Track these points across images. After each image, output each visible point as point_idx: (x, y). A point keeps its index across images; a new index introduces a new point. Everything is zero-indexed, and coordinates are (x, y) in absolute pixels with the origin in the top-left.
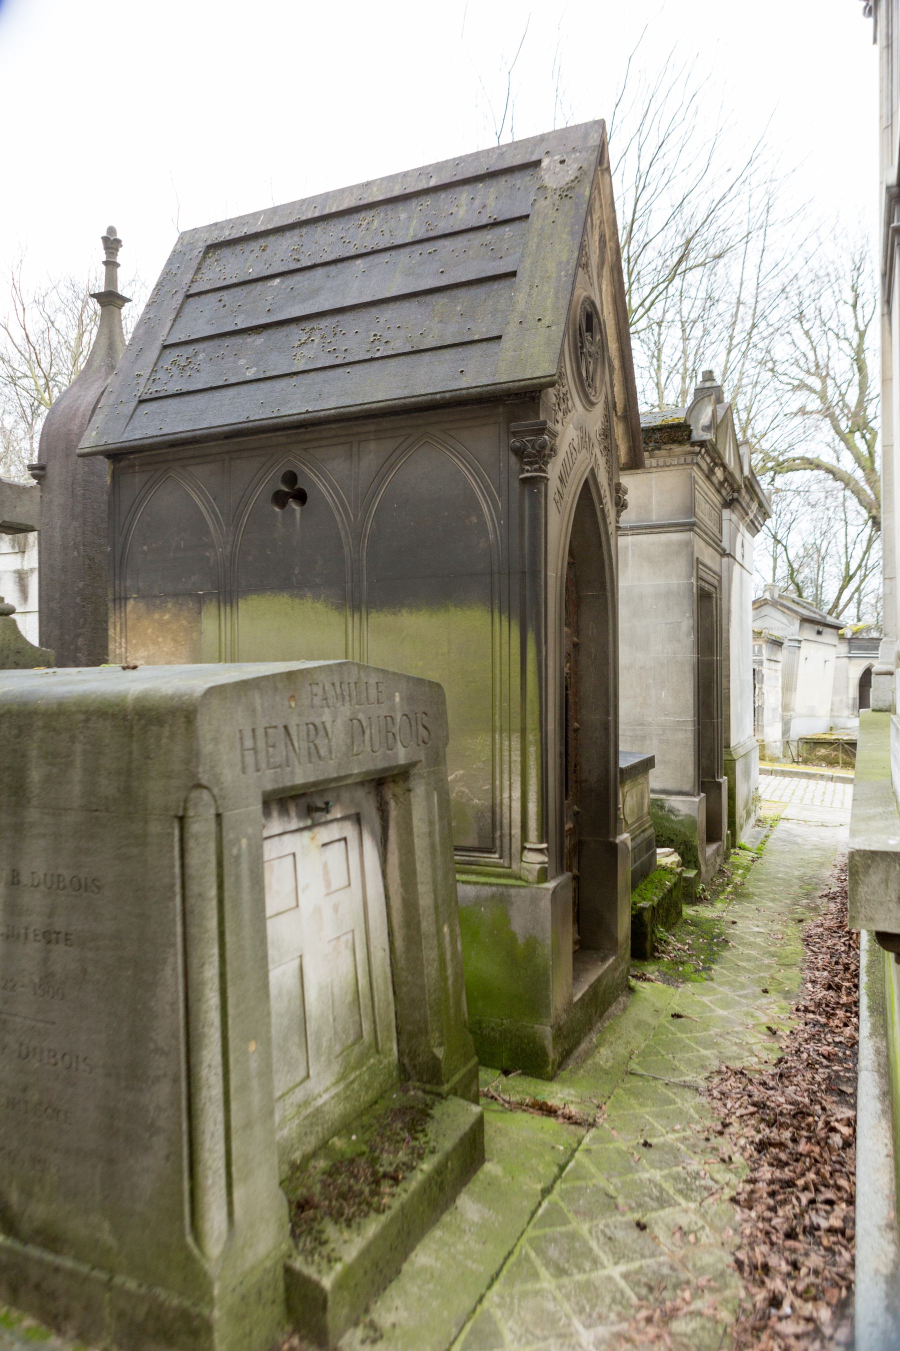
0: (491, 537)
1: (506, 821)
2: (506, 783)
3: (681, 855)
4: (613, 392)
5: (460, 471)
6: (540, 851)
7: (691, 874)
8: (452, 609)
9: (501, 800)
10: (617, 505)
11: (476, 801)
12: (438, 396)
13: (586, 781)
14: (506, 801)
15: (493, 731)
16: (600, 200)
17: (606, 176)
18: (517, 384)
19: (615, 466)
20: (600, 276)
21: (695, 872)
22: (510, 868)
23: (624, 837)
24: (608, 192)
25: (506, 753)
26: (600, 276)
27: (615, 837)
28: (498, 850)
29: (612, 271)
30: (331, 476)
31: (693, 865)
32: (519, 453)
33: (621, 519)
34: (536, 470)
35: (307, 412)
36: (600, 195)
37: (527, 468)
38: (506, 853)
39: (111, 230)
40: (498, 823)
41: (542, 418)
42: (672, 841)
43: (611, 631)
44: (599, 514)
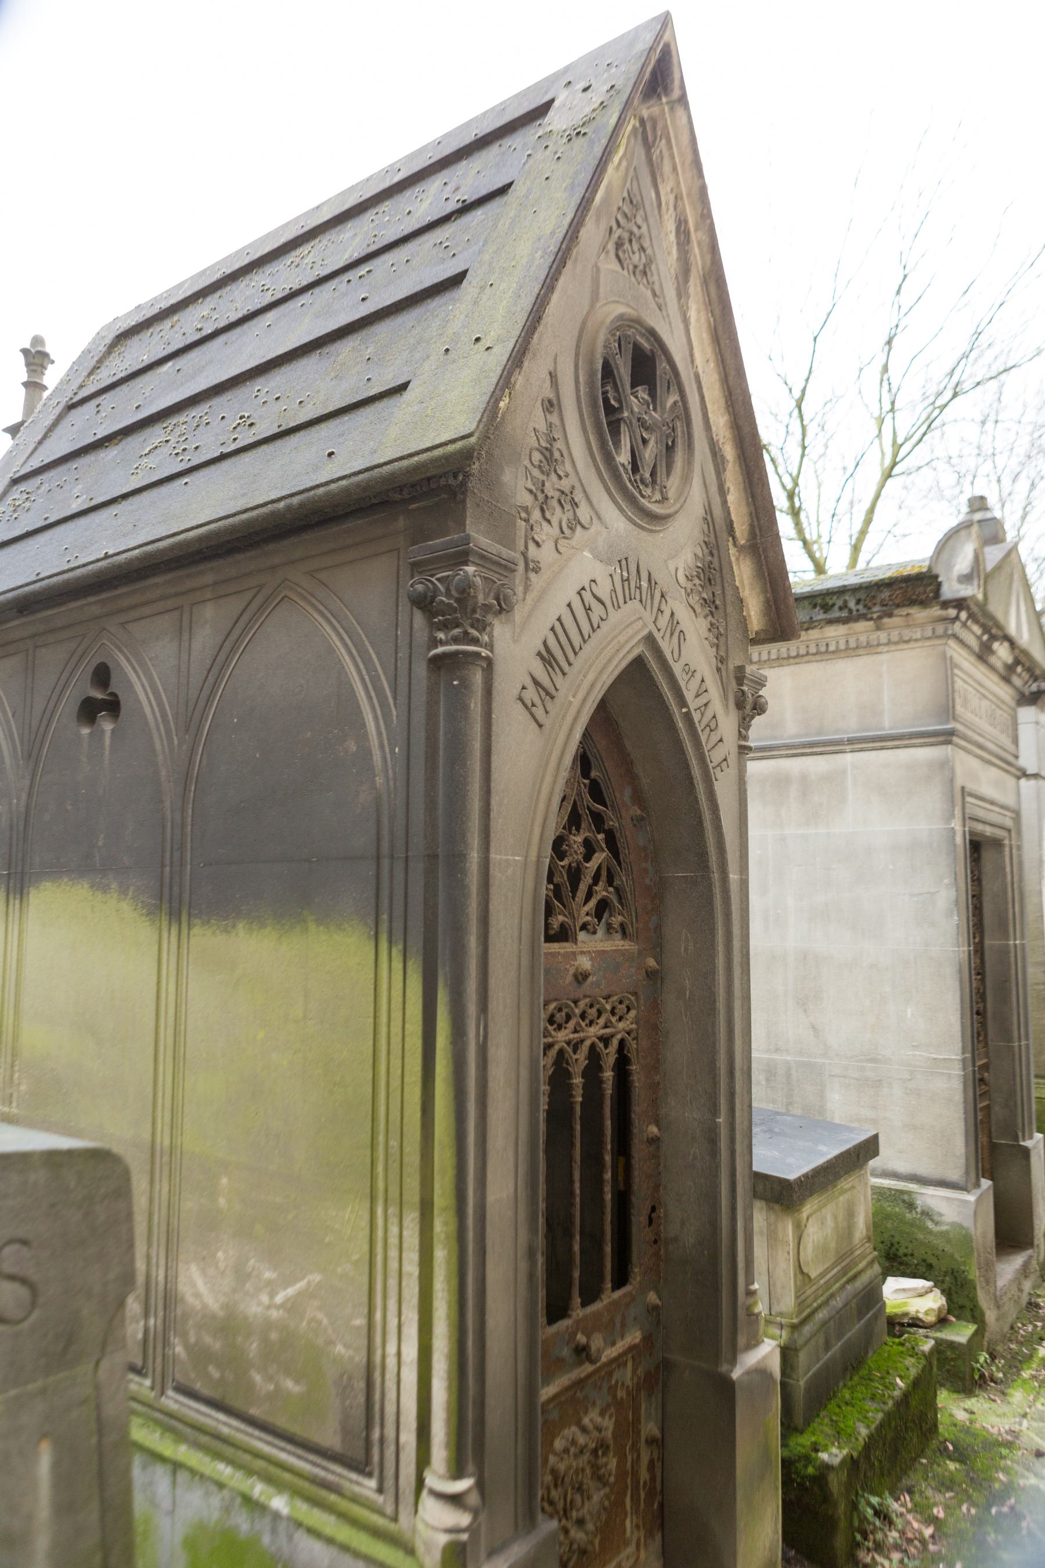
0: (379, 780)
1: (390, 1409)
2: (393, 1322)
3: (947, 1293)
4: (725, 502)
5: (334, 649)
6: (455, 1500)
7: (961, 1333)
8: (312, 926)
9: (384, 1357)
10: (740, 705)
11: (339, 1349)
12: (282, 504)
13: (676, 1239)
14: (391, 1362)
15: (373, 1199)
16: (672, 157)
17: (680, 112)
18: (405, 463)
19: (734, 636)
20: (682, 293)
21: (972, 1328)
22: (395, 1519)
23: (765, 1353)
24: (685, 139)
25: (393, 1253)
26: (682, 293)
27: (733, 1362)
28: (376, 1473)
29: (705, 283)
30: (152, 671)
31: (968, 1314)
32: (424, 603)
33: (752, 733)
34: (456, 640)
35: (107, 556)
36: (670, 148)
37: (441, 635)
38: (389, 1483)
39: (37, 340)
40: (377, 1407)
41: (467, 532)
42: (930, 1266)
43: (721, 948)
44: (680, 724)
